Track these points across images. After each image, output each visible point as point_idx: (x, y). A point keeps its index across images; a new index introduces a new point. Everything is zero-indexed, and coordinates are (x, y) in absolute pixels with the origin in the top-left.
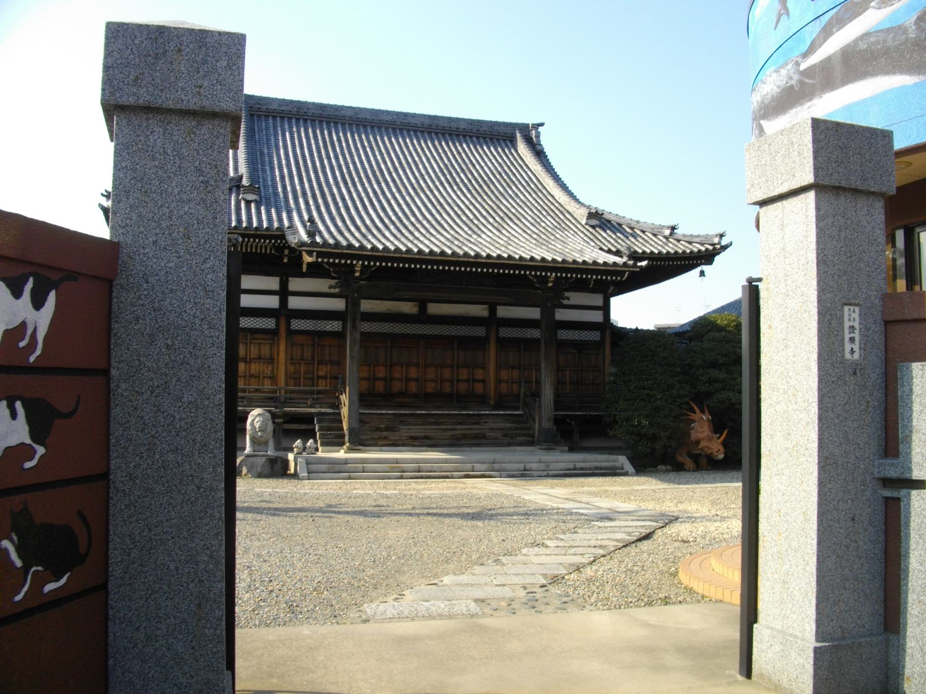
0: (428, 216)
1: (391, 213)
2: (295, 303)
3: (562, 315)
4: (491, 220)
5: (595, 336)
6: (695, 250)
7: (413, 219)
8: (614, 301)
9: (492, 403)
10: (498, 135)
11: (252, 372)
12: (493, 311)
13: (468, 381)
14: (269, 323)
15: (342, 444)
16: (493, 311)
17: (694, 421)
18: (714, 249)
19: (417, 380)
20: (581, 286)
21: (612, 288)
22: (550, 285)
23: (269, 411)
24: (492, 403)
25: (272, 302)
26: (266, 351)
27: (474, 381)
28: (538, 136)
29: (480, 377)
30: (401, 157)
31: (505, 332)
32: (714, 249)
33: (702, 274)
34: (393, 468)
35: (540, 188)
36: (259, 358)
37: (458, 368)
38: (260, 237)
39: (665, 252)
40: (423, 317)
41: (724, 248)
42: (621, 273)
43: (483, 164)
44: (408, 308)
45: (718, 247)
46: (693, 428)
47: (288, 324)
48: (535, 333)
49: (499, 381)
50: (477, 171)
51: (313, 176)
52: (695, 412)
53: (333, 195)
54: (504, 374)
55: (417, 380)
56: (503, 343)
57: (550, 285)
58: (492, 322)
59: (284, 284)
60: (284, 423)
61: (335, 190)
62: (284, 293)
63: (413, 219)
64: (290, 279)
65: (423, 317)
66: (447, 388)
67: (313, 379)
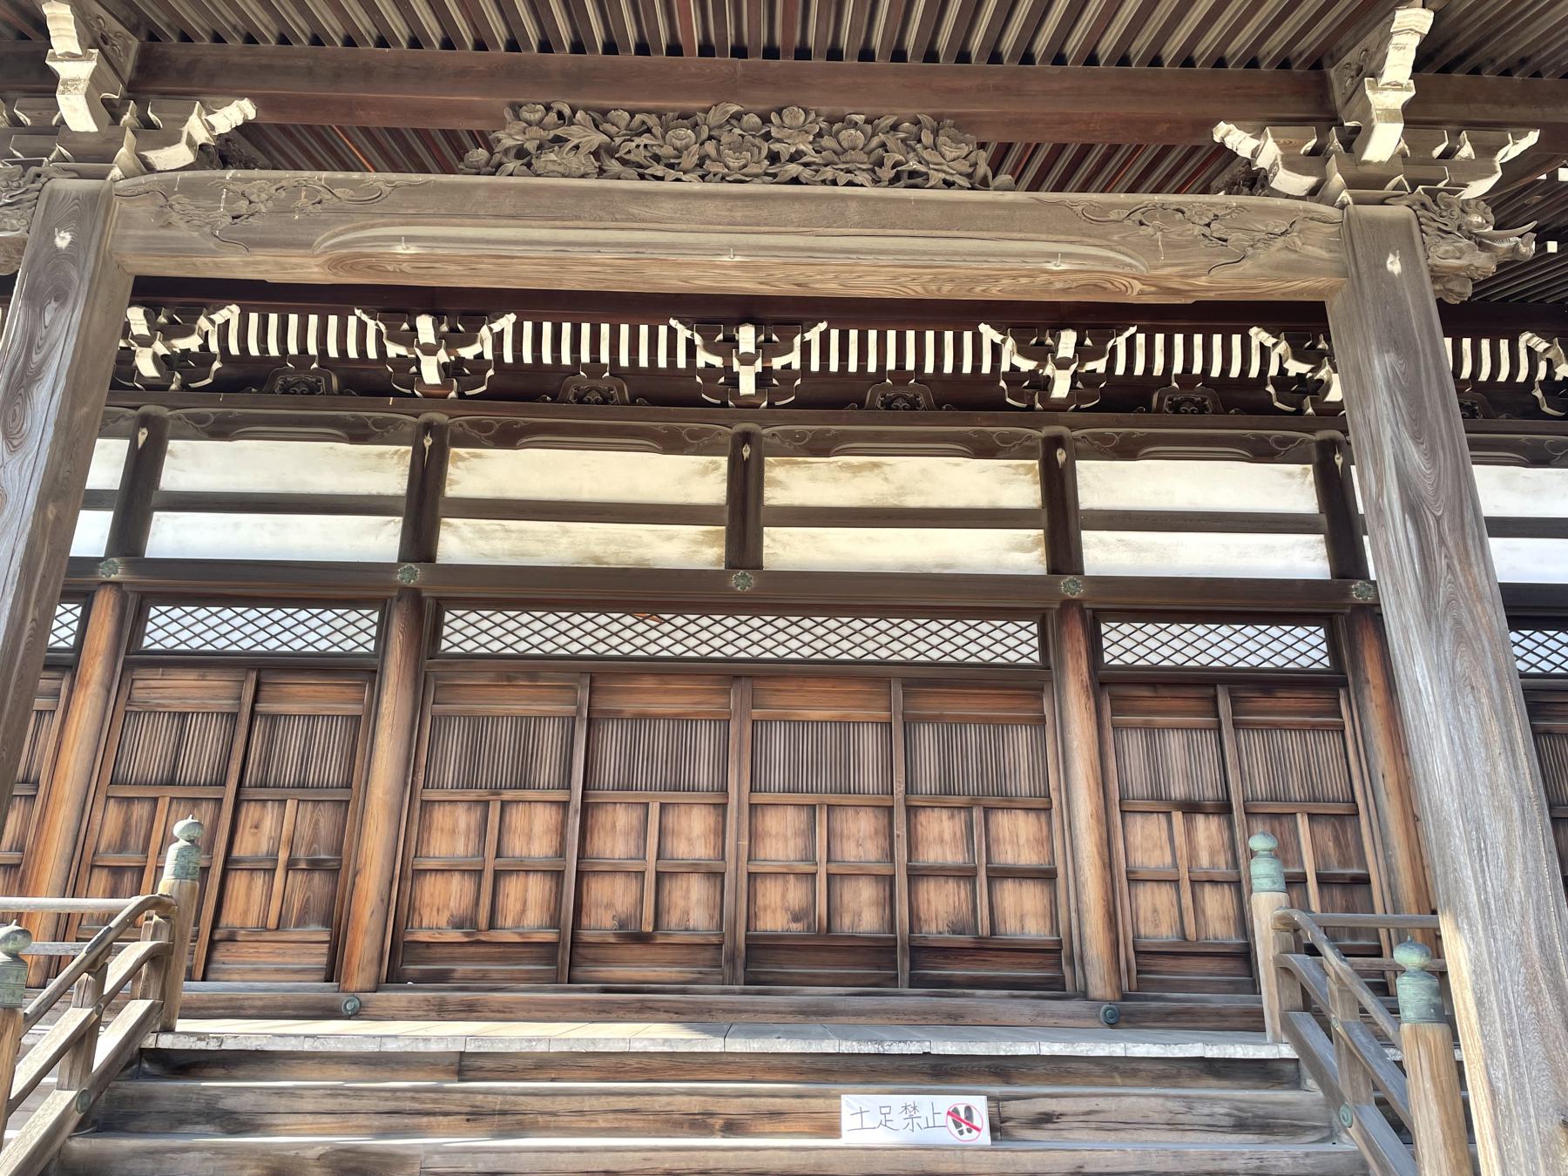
9: (1099, 981)
13: (965, 874)
24: (1099, 981)
27: (999, 874)
29: (1028, 857)
31: (1127, 645)
37: (911, 811)
40: (741, 584)
49: (1122, 879)
54: (1149, 841)
55: (715, 876)
64: (173, 445)
66: (862, 912)
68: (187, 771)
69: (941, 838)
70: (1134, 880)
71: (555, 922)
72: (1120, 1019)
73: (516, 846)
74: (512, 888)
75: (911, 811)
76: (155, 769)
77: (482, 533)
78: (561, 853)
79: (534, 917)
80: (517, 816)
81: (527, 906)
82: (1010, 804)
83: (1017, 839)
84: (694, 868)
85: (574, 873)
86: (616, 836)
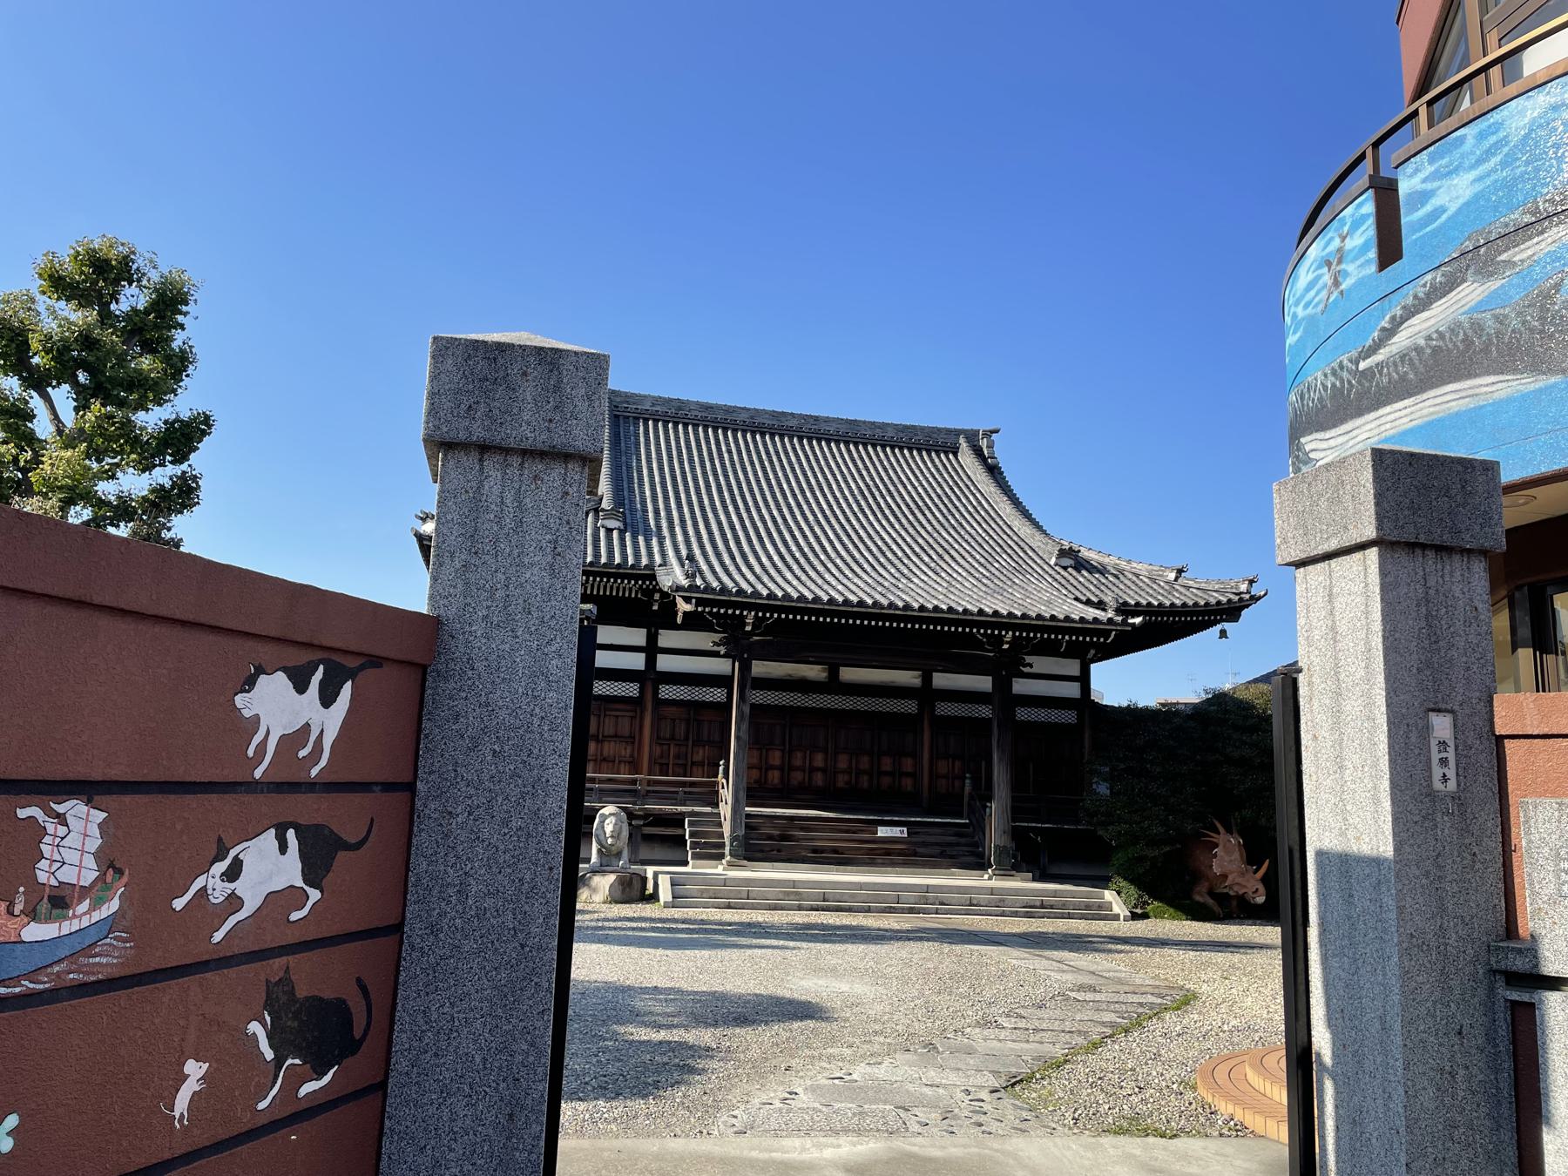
0: (843, 553)
1: (794, 548)
2: (665, 663)
3: (1020, 686)
4: (926, 559)
5: (1069, 717)
6: (1213, 601)
7: (823, 557)
8: (1095, 668)
10: (939, 443)
11: (605, 753)
12: (927, 679)
14: (631, 689)
15: (721, 857)
16: (927, 679)
17: (1216, 846)
18: (1241, 600)
19: (824, 770)
20: (1049, 649)
21: (1093, 652)
22: (1006, 646)
25: (637, 661)
26: (625, 727)
28: (990, 446)
29: (910, 770)
30: (809, 474)
32: (1241, 600)
33: (1223, 634)
34: (788, 893)
35: (994, 517)
36: (616, 736)
38: (623, 576)
39: (1168, 603)
40: (833, 685)
41: (1255, 599)
42: (1107, 633)
44: (814, 672)
48: (985, 711)
51: (694, 498)
53: (719, 523)
54: (943, 767)
55: (824, 770)
57: (1006, 646)
58: (926, 694)
59: (652, 639)
61: (723, 517)
62: (651, 650)
63: (823, 557)
65: (833, 685)
69: (887, 764)
74: (770, 773)
83: (908, 765)
85: (786, 769)
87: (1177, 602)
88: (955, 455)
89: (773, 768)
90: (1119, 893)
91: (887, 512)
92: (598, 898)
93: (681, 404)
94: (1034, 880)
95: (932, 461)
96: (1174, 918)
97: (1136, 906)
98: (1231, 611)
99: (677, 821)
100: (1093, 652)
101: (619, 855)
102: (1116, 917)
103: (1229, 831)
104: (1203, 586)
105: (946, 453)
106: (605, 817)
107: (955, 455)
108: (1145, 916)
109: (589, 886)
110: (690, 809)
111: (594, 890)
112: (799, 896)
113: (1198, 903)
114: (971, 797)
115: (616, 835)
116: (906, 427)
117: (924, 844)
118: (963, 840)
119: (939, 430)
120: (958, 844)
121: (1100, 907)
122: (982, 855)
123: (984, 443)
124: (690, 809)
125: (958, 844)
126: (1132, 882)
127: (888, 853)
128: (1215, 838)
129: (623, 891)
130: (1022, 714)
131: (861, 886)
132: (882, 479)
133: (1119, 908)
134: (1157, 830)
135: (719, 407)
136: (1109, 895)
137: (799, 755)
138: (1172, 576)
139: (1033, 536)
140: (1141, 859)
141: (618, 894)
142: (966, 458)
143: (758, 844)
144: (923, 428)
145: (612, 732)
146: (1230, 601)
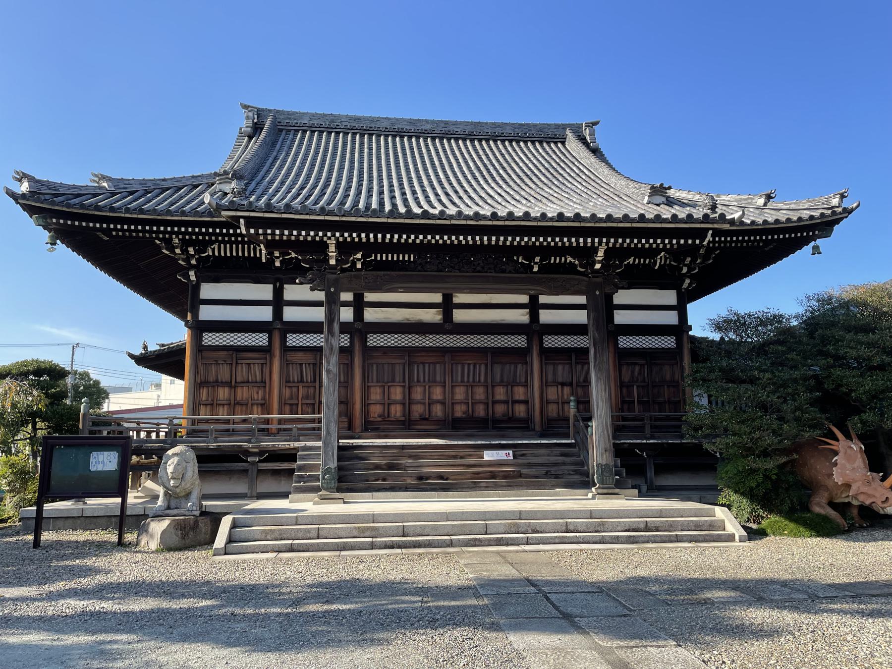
5: (668, 342)
9: (538, 428)
10: (550, 136)
11: (239, 398)
13: (506, 402)
14: (260, 339)
17: (836, 453)
18: (834, 213)
21: (687, 281)
22: (598, 266)
23: (192, 447)
24: (538, 428)
25: (265, 314)
26: (256, 373)
27: (515, 402)
29: (522, 398)
31: (550, 341)
32: (834, 213)
36: (248, 382)
37: (493, 387)
40: (447, 326)
41: (848, 212)
43: (527, 162)
45: (840, 209)
46: (836, 464)
47: (284, 340)
50: (521, 168)
52: (838, 440)
54: (552, 393)
55: (443, 403)
56: (549, 354)
57: (598, 266)
59: (278, 293)
60: (260, 461)
64: (285, 286)
65: (447, 326)
66: (480, 411)
67: (314, 404)
68: (305, 379)
69: (500, 393)
70: (548, 402)
71: (404, 415)
72: (542, 436)
73: (393, 397)
74: (393, 407)
75: (493, 387)
76: (296, 378)
77: (376, 312)
78: (404, 398)
79: (399, 414)
80: (392, 390)
81: (397, 411)
82: (518, 384)
83: (520, 393)
84: (438, 402)
85: (408, 403)
86: (418, 394)
87: (770, 220)
88: (563, 143)
89: (395, 403)
90: (729, 507)
91: (498, 178)
92: (154, 545)
93: (333, 118)
94: (641, 495)
95: (544, 149)
96: (795, 535)
97: (749, 521)
98: (824, 226)
99: (291, 456)
100: (687, 281)
101: (188, 496)
102: (731, 538)
103: (848, 437)
104: (793, 206)
105: (556, 143)
106: (169, 458)
107: (563, 143)
108: (761, 534)
109: (147, 531)
110: (302, 444)
111: (152, 536)
112: (375, 532)
113: (819, 515)
114: (576, 419)
115: (180, 475)
116: (521, 125)
117: (530, 465)
118: (568, 460)
119: (549, 125)
120: (564, 464)
121: (711, 526)
122: (587, 474)
123: (586, 133)
124: (302, 444)
125: (564, 464)
126: (743, 494)
127: (493, 476)
128: (834, 445)
129: (183, 537)
130: (625, 342)
131: (447, 516)
132: (498, 161)
133: (733, 527)
134: (769, 440)
135: (365, 119)
136: (720, 513)
137: (419, 390)
138: (761, 201)
139: (627, 186)
140: (753, 471)
141: (175, 540)
142: (573, 144)
143: (349, 477)
144: (535, 125)
145: (244, 379)
146: (822, 214)
